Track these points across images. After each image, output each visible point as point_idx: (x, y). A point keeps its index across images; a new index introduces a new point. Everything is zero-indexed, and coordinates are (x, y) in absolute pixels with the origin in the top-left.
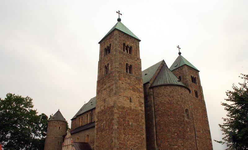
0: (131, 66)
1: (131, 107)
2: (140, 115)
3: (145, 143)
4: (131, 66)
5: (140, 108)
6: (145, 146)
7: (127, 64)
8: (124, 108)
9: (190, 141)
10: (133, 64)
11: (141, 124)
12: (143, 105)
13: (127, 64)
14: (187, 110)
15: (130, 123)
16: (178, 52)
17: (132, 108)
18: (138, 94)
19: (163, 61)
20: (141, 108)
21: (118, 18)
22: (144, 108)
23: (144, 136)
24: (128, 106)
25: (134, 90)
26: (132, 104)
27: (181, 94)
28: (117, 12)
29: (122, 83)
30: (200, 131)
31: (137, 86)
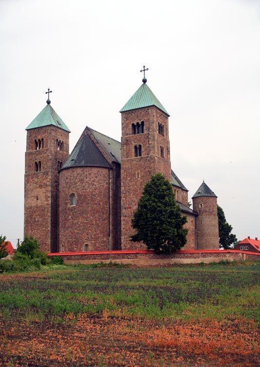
0: (40, 162)
1: (37, 205)
2: (46, 209)
3: (49, 235)
4: (40, 162)
5: (46, 203)
6: (50, 237)
7: (36, 163)
8: (31, 207)
9: (70, 229)
10: (41, 160)
11: (46, 217)
12: (50, 199)
13: (36, 163)
14: (73, 195)
15: (37, 220)
16: (143, 78)
17: (39, 205)
18: (44, 190)
19: (87, 129)
20: (47, 202)
21: (47, 100)
22: (50, 201)
23: (49, 228)
24: (35, 205)
25: (41, 187)
26: (39, 201)
27: (67, 178)
28: (49, 90)
29: (30, 185)
30: (130, 208)
31: (45, 181)
